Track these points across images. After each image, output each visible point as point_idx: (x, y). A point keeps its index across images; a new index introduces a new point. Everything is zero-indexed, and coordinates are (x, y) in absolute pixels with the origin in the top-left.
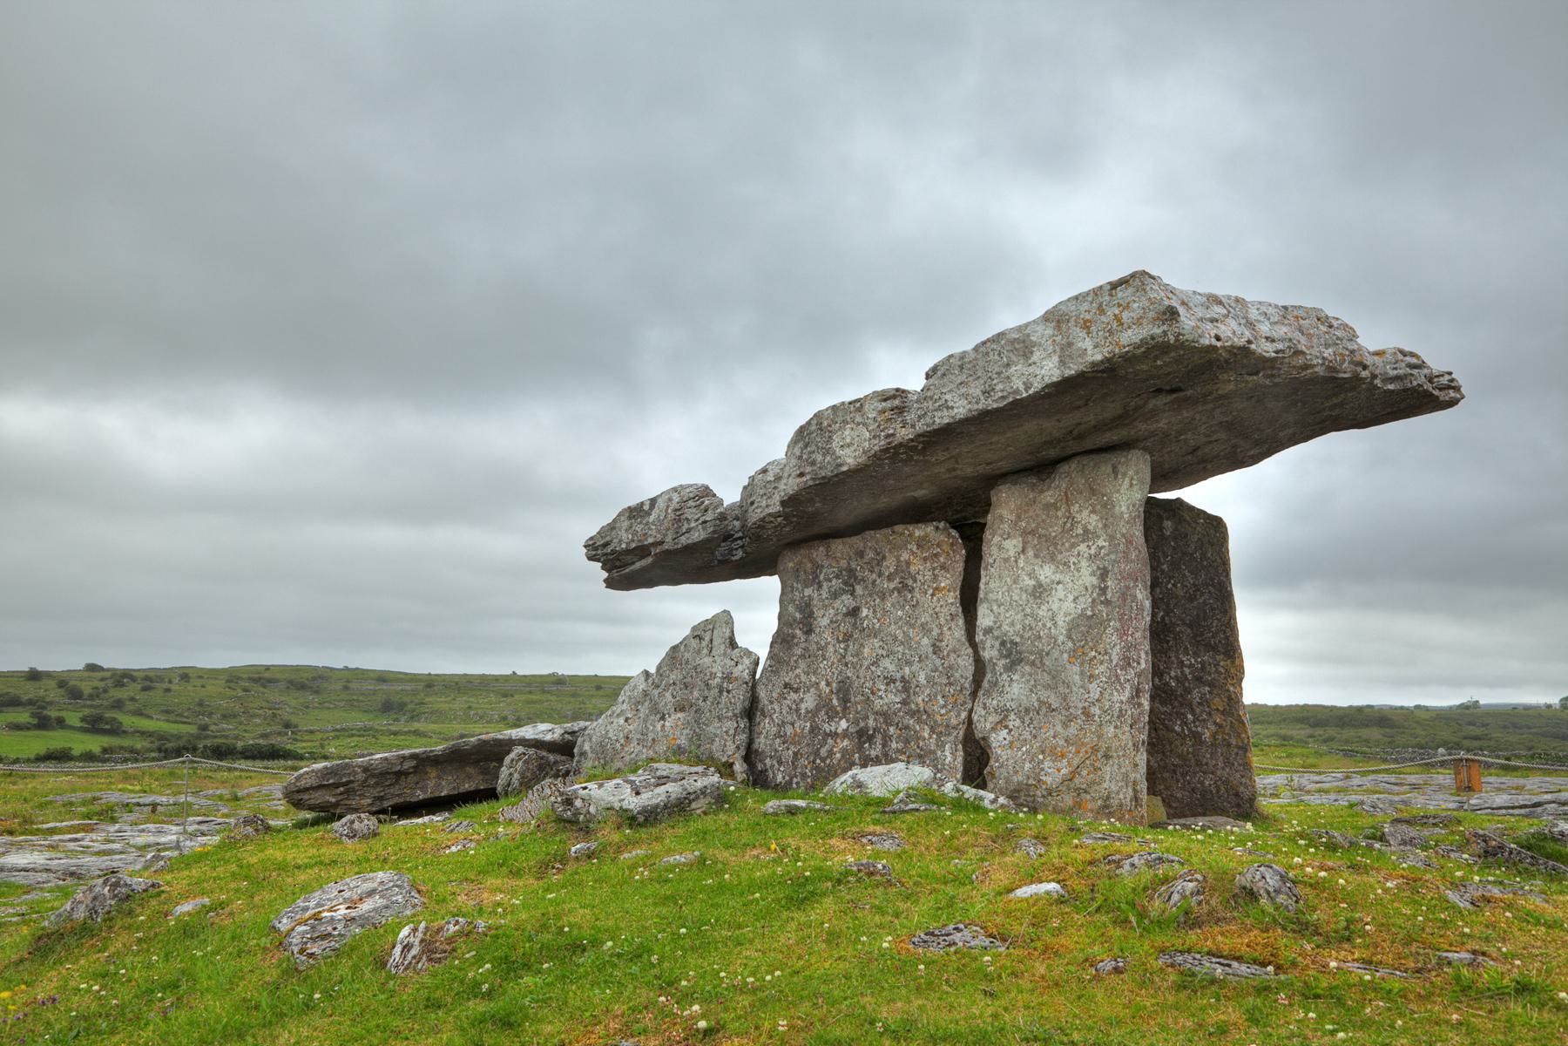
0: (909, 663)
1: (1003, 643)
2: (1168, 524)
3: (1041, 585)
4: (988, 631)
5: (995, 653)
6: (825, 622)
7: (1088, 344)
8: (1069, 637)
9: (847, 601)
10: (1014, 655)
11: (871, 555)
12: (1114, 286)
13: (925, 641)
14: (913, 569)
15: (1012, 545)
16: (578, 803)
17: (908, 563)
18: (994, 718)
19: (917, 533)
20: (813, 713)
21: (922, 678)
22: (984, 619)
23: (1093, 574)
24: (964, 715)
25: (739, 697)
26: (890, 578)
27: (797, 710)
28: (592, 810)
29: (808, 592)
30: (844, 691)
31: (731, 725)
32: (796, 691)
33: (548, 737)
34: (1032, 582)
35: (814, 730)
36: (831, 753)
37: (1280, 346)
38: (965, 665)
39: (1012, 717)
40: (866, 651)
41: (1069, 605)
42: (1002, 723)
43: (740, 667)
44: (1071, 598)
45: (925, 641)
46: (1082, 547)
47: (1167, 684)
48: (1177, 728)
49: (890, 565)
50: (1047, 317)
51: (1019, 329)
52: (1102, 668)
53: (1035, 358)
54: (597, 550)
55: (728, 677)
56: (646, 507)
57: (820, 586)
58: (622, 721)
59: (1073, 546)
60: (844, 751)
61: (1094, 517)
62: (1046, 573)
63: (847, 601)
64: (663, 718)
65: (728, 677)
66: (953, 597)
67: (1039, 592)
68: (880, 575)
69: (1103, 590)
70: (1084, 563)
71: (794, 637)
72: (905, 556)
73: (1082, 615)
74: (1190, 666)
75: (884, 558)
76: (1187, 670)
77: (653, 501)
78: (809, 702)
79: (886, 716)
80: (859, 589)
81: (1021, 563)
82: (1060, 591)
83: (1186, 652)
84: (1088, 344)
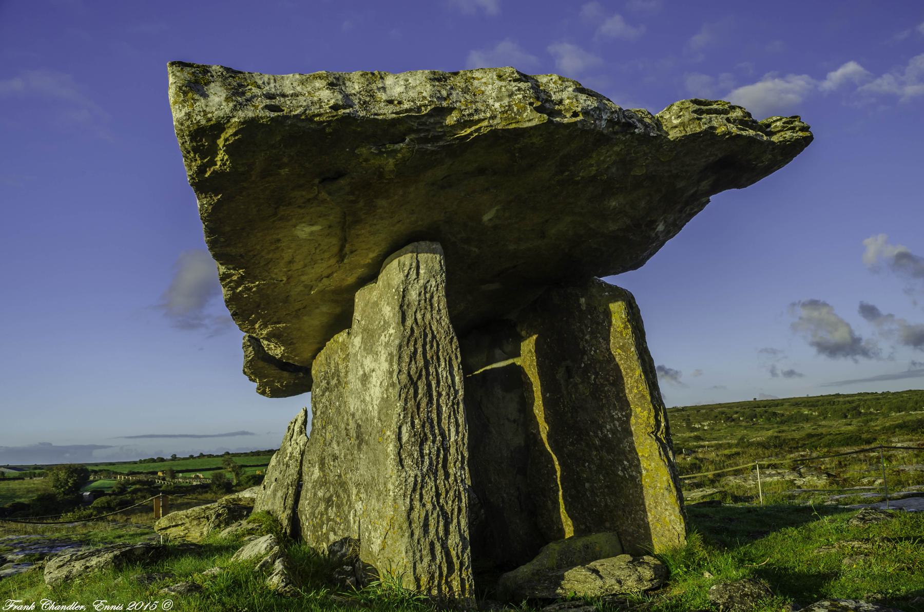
2: (583, 300)
8: (379, 419)
19: (341, 340)
23: (386, 361)
25: (293, 471)
26: (333, 379)
34: (361, 373)
37: (406, 106)
39: (362, 490)
45: (343, 426)
46: (383, 337)
47: (606, 436)
48: (620, 473)
59: (379, 337)
61: (389, 309)
73: (383, 398)
74: (619, 419)
76: (617, 423)
83: (615, 408)
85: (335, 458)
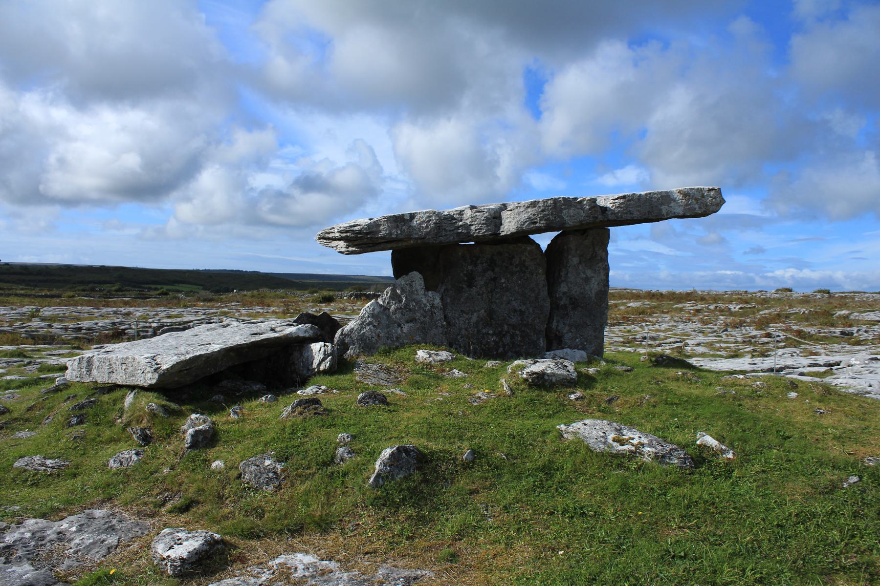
0: (524, 304)
1: (571, 299)
3: (587, 277)
4: (565, 293)
5: (567, 302)
6: (483, 283)
7: (697, 206)
9: (489, 274)
10: (575, 303)
11: (507, 255)
12: (710, 190)
13: (533, 295)
14: (527, 264)
15: (575, 260)
16: (546, 377)
17: (524, 261)
20: (477, 323)
21: (531, 310)
22: (563, 288)
28: (554, 380)
29: (470, 267)
30: (491, 313)
32: (467, 314)
35: (479, 331)
36: (488, 343)
38: (548, 304)
40: (505, 298)
41: (596, 286)
45: (533, 295)
46: (600, 264)
49: (516, 261)
50: (680, 192)
51: (666, 192)
53: (672, 204)
55: (433, 306)
56: (408, 218)
57: (476, 265)
60: (494, 341)
62: (589, 273)
63: (489, 274)
64: (399, 325)
65: (433, 306)
66: (543, 277)
67: (587, 280)
68: (511, 264)
70: (602, 271)
71: (463, 288)
72: (523, 258)
73: (601, 291)
75: (513, 257)
77: (412, 216)
78: (474, 318)
79: (514, 327)
80: (497, 269)
81: (580, 267)
82: (593, 280)
84: (697, 206)
85: (515, 311)
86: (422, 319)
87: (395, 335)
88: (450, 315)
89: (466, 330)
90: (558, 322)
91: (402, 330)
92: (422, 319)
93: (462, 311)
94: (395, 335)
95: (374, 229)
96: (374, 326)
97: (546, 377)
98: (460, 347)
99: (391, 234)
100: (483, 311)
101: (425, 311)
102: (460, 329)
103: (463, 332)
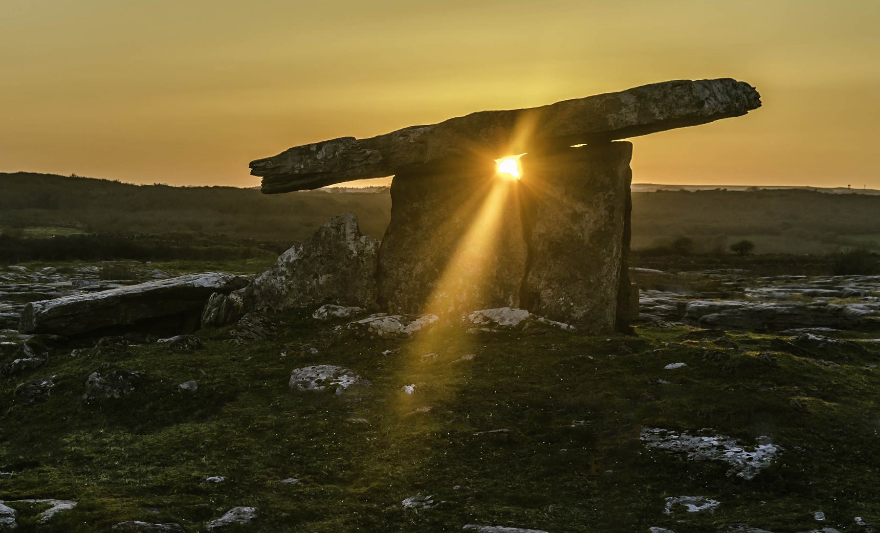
16: (370, 330)
18: (543, 283)
24: (520, 279)
27: (410, 274)
28: (380, 333)
31: (365, 282)
33: (217, 286)
34: (571, 212)
42: (548, 286)
43: (368, 248)
44: (592, 221)
52: (609, 259)
54: (256, 168)
55: (361, 253)
56: (314, 149)
58: (284, 278)
65: (361, 253)
69: (611, 218)
77: (320, 146)
86: (344, 268)
87: (308, 288)
88: (385, 264)
89: (406, 282)
90: (533, 274)
91: (317, 282)
92: (344, 268)
93: (402, 260)
94: (308, 288)
95: (279, 165)
96: (287, 277)
97: (370, 330)
98: (398, 304)
99: (293, 168)
100: (428, 260)
101: (349, 259)
102: (399, 282)
103: (403, 285)
